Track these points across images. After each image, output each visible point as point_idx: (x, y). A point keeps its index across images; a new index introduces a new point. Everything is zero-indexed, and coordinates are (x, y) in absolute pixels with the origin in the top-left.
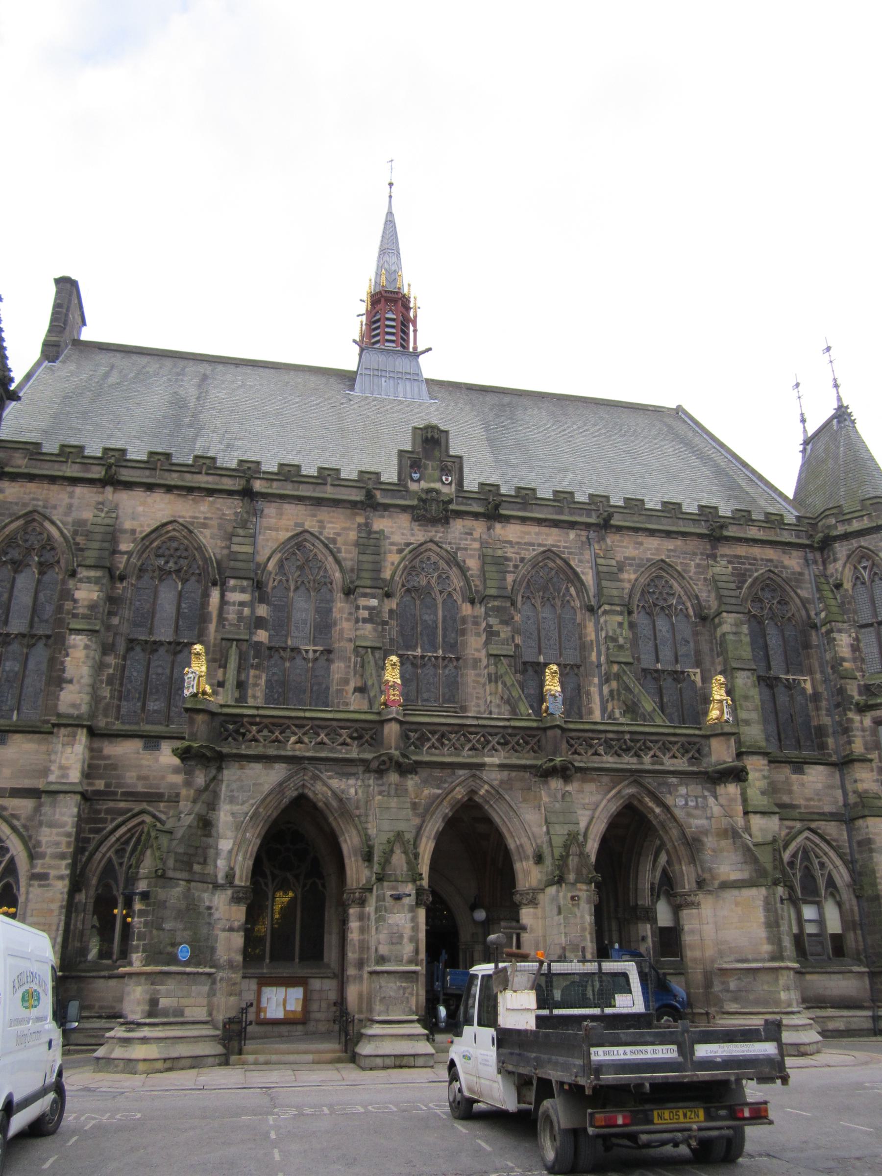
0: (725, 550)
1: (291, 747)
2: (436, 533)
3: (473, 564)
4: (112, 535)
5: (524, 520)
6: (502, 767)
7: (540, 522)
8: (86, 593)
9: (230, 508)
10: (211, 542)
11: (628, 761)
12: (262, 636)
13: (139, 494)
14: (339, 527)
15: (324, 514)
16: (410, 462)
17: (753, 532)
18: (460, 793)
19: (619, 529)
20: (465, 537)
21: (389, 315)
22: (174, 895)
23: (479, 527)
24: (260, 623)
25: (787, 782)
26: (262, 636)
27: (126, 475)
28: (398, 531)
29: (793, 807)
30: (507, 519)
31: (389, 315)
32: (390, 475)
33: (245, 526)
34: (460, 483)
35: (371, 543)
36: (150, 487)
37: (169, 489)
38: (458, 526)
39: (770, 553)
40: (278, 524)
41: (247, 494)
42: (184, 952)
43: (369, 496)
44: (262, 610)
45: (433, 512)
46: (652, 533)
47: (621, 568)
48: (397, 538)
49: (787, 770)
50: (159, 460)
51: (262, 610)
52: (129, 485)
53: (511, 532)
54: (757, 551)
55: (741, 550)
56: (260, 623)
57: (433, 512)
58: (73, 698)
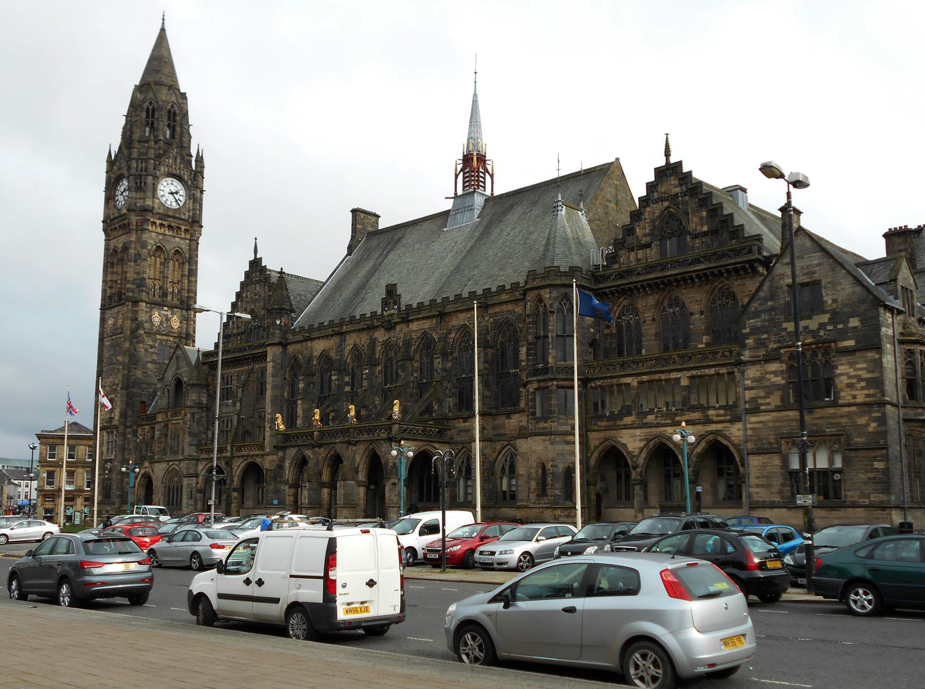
0: (491, 311)
1: (299, 442)
2: (392, 334)
4: (310, 359)
5: (418, 319)
6: (340, 442)
7: (423, 318)
8: (301, 385)
10: (333, 354)
11: (371, 437)
12: (347, 389)
13: (317, 341)
14: (363, 340)
16: (385, 303)
17: (504, 297)
18: (332, 452)
19: (450, 313)
20: (400, 332)
21: (473, 165)
22: (272, 486)
23: (403, 326)
24: (347, 384)
25: (504, 424)
26: (347, 389)
27: (314, 335)
29: (504, 435)
30: (412, 321)
31: (473, 165)
32: (379, 312)
33: (340, 348)
34: (399, 308)
35: (373, 342)
36: (318, 338)
37: (323, 337)
38: (398, 328)
39: (510, 307)
40: (351, 340)
41: (341, 334)
42: (275, 502)
44: (347, 379)
46: (462, 311)
47: (449, 332)
48: (381, 340)
49: (504, 417)
51: (347, 379)
52: (314, 339)
53: (414, 326)
54: (504, 308)
55: (497, 309)
56: (347, 384)
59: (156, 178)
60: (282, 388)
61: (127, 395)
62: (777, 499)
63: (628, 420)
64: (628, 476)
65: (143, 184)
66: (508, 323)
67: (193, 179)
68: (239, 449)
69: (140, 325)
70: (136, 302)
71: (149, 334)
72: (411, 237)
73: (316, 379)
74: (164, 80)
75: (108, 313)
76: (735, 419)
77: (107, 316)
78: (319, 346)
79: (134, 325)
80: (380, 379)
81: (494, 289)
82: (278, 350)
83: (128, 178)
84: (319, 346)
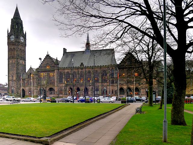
3: (84, 72)
8: (63, 76)
9: (71, 70)
14: (76, 71)
15: (76, 70)
16: (81, 65)
20: (84, 70)
21: (88, 44)
28: (80, 70)
35: (78, 71)
38: (83, 69)
43: (78, 68)
45: (82, 69)
50: (67, 68)
57: (82, 69)
58: (63, 82)
59: (20, 36)
60: (58, 76)
61: (17, 76)
62: (145, 94)
63: (124, 84)
64: (124, 91)
65: (17, 37)
66: (104, 71)
67: (25, 36)
68: (48, 85)
69: (19, 63)
70: (18, 59)
71: (20, 65)
72: (77, 54)
73: (66, 75)
74: (19, 18)
75: (10, 60)
76: (140, 85)
77: (9, 60)
78: (66, 71)
79: (17, 63)
80: (80, 76)
81: (102, 66)
82: (57, 70)
83: (15, 36)
84: (66, 71)
